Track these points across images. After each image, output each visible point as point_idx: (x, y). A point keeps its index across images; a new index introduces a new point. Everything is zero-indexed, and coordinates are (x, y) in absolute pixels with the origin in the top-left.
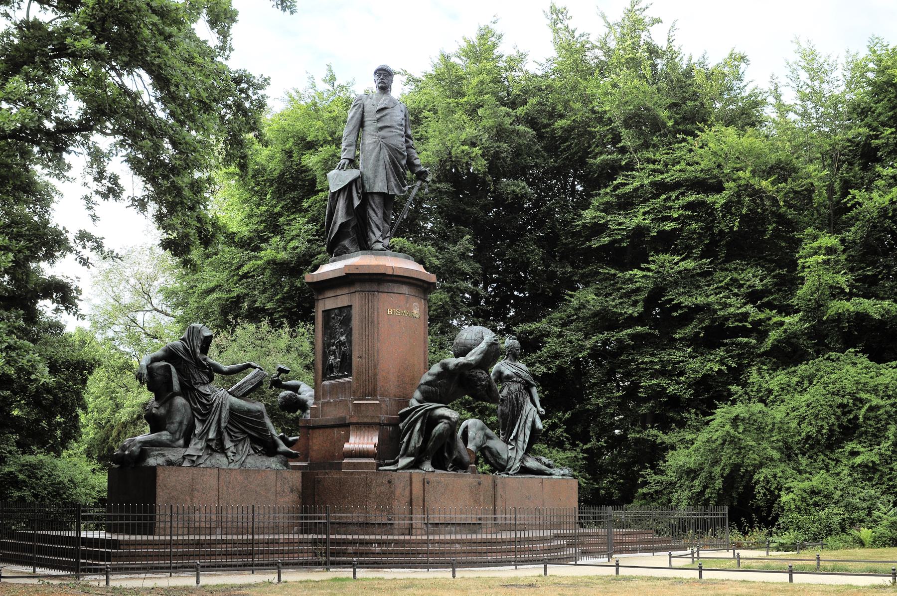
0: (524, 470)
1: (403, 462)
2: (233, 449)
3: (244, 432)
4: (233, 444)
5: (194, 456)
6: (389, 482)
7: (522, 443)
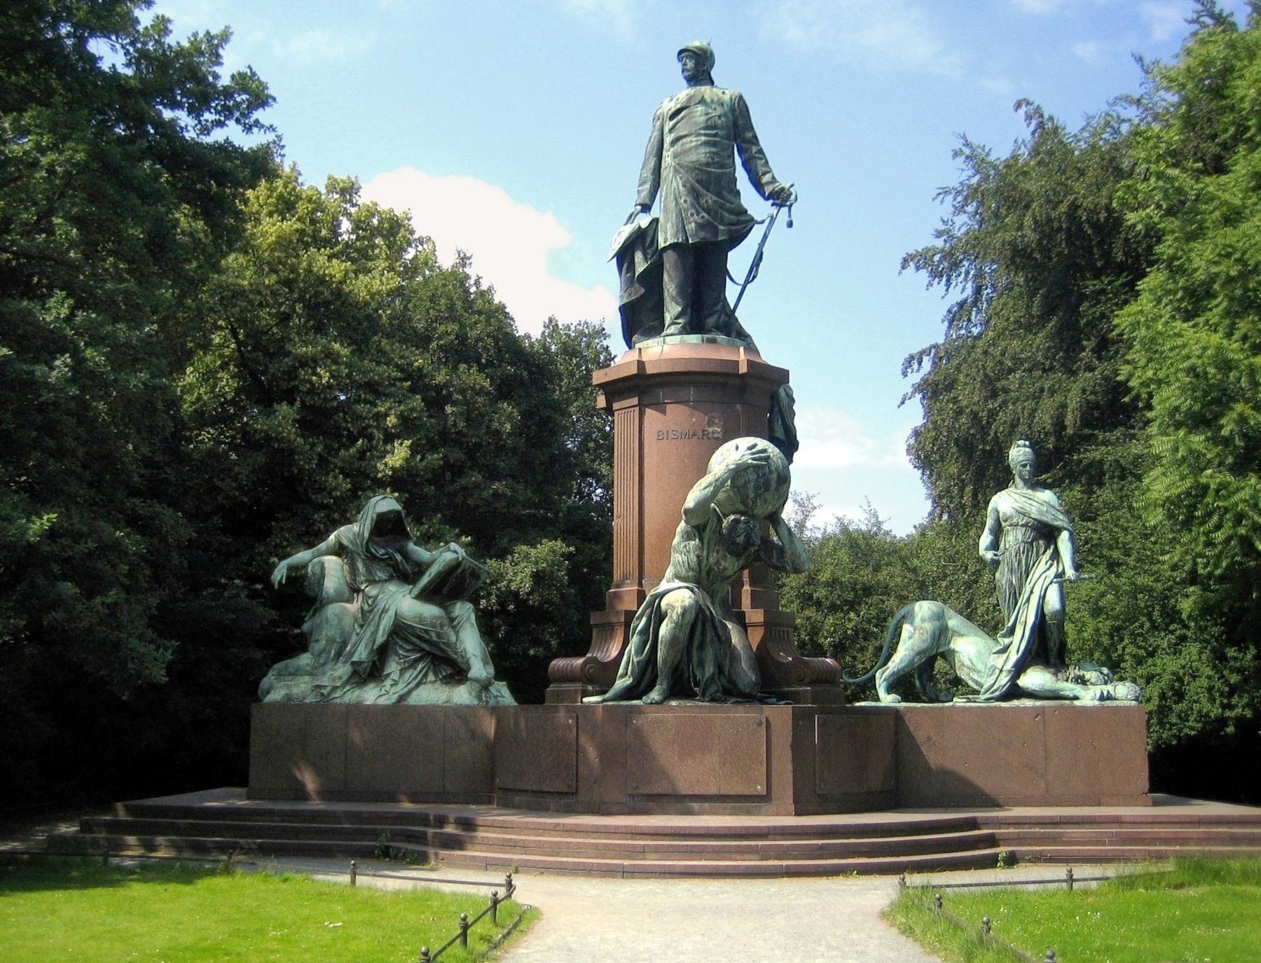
1: (621, 683)
2: (395, 676)
3: (418, 649)
4: (399, 668)
5: (325, 687)
7: (1019, 642)
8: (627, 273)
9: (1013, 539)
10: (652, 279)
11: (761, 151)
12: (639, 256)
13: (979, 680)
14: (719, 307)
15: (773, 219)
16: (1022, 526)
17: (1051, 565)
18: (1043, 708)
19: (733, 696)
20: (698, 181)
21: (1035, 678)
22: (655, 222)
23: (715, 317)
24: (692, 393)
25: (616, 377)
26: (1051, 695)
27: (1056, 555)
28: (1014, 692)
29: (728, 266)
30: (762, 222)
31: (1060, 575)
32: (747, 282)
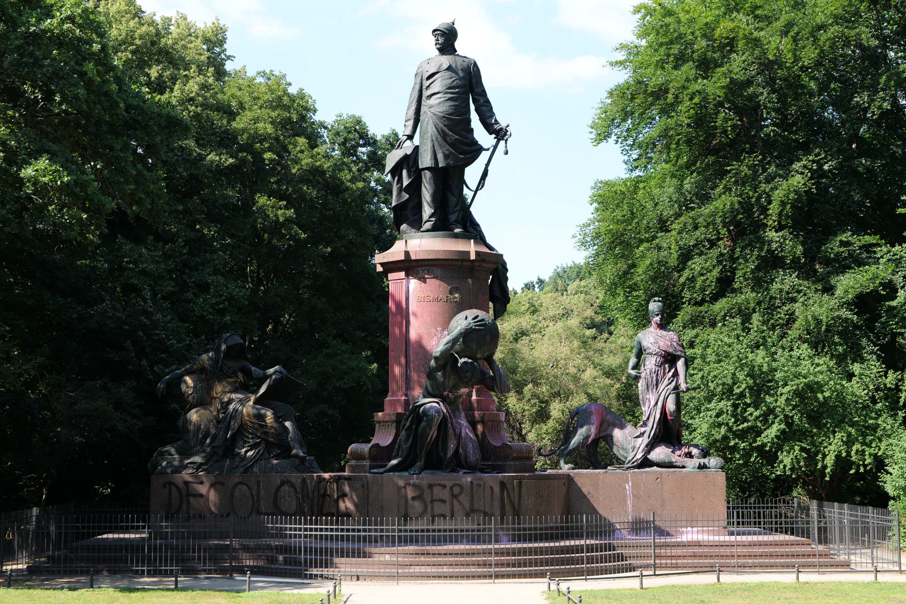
0: (646, 463)
6: (363, 486)
7: (650, 429)
8: (397, 184)
9: (651, 363)
10: (415, 188)
11: (488, 101)
12: (405, 172)
13: (625, 454)
14: (458, 208)
15: (495, 147)
16: (655, 354)
17: (673, 381)
18: (661, 473)
19: (465, 469)
20: (445, 126)
21: (660, 453)
22: (417, 148)
23: (456, 214)
24: (438, 271)
25: (391, 260)
27: (676, 374)
28: (646, 463)
29: (466, 178)
30: (488, 150)
31: (676, 388)
32: (477, 189)
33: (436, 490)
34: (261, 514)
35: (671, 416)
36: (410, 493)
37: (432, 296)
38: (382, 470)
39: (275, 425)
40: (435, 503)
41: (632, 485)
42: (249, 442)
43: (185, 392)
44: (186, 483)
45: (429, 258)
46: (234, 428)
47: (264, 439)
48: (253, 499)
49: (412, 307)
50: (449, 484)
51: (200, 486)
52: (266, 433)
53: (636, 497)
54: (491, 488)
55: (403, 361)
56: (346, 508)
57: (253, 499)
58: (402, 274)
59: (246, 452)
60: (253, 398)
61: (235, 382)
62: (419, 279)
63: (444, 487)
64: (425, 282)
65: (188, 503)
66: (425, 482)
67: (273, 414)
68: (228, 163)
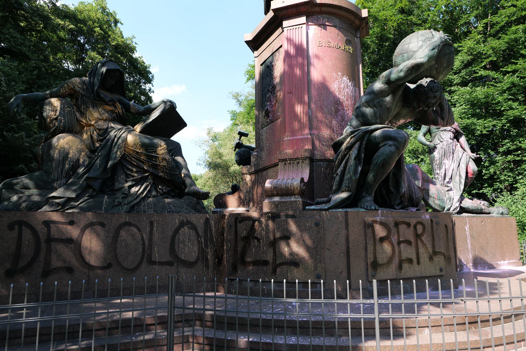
0: (463, 210)
6: (317, 225)
13: (441, 204)
24: (337, 21)
26: (479, 212)
33: (402, 227)
34: (154, 263)
35: (473, 175)
36: (380, 232)
37: (333, 43)
38: (325, 206)
39: (167, 157)
40: (402, 245)
41: (469, 227)
42: (133, 176)
43: (48, 117)
44: (48, 223)
45: (334, 3)
46: (115, 158)
47: (151, 174)
48: (144, 244)
49: (312, 51)
50: (413, 222)
51: (69, 227)
52: (155, 167)
53: (472, 237)
54: (446, 226)
55: (306, 98)
56: (292, 254)
57: (144, 244)
58: (303, 19)
59: (130, 187)
60: (138, 128)
61: (112, 112)
62: (319, 25)
63: (408, 225)
64: (326, 29)
65: (49, 251)
66: (391, 221)
67: (166, 144)
68: (70, 27)
